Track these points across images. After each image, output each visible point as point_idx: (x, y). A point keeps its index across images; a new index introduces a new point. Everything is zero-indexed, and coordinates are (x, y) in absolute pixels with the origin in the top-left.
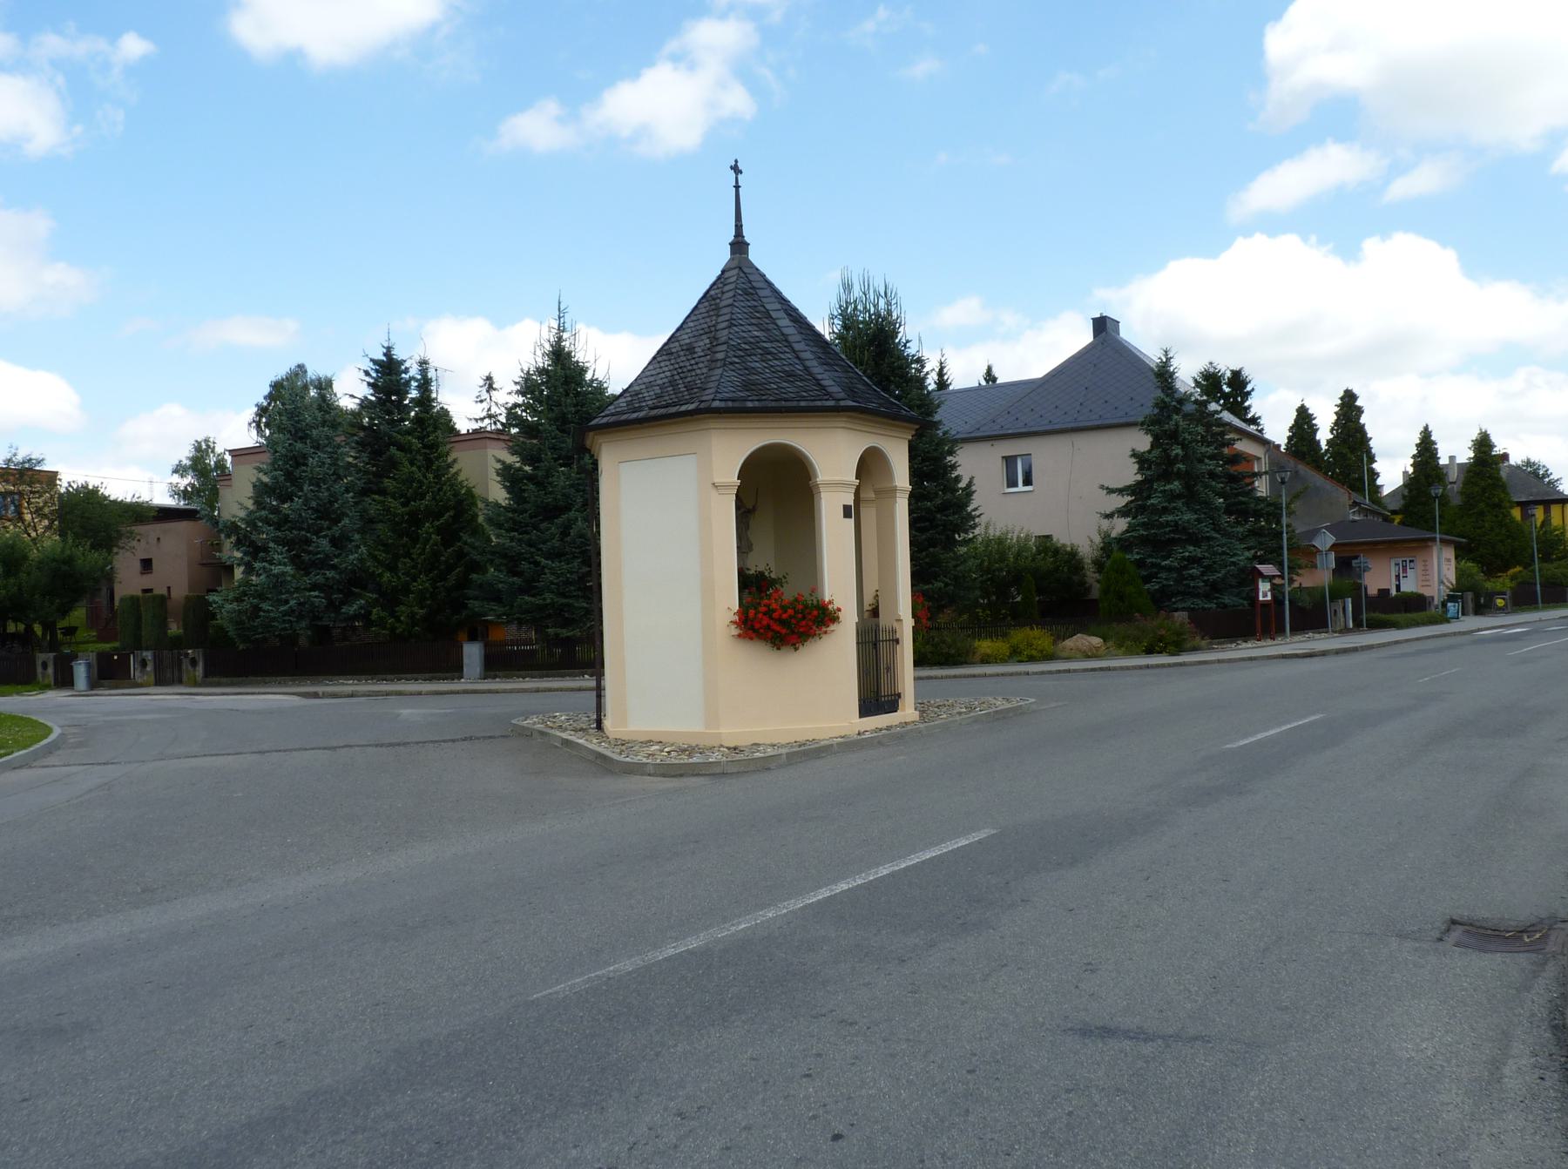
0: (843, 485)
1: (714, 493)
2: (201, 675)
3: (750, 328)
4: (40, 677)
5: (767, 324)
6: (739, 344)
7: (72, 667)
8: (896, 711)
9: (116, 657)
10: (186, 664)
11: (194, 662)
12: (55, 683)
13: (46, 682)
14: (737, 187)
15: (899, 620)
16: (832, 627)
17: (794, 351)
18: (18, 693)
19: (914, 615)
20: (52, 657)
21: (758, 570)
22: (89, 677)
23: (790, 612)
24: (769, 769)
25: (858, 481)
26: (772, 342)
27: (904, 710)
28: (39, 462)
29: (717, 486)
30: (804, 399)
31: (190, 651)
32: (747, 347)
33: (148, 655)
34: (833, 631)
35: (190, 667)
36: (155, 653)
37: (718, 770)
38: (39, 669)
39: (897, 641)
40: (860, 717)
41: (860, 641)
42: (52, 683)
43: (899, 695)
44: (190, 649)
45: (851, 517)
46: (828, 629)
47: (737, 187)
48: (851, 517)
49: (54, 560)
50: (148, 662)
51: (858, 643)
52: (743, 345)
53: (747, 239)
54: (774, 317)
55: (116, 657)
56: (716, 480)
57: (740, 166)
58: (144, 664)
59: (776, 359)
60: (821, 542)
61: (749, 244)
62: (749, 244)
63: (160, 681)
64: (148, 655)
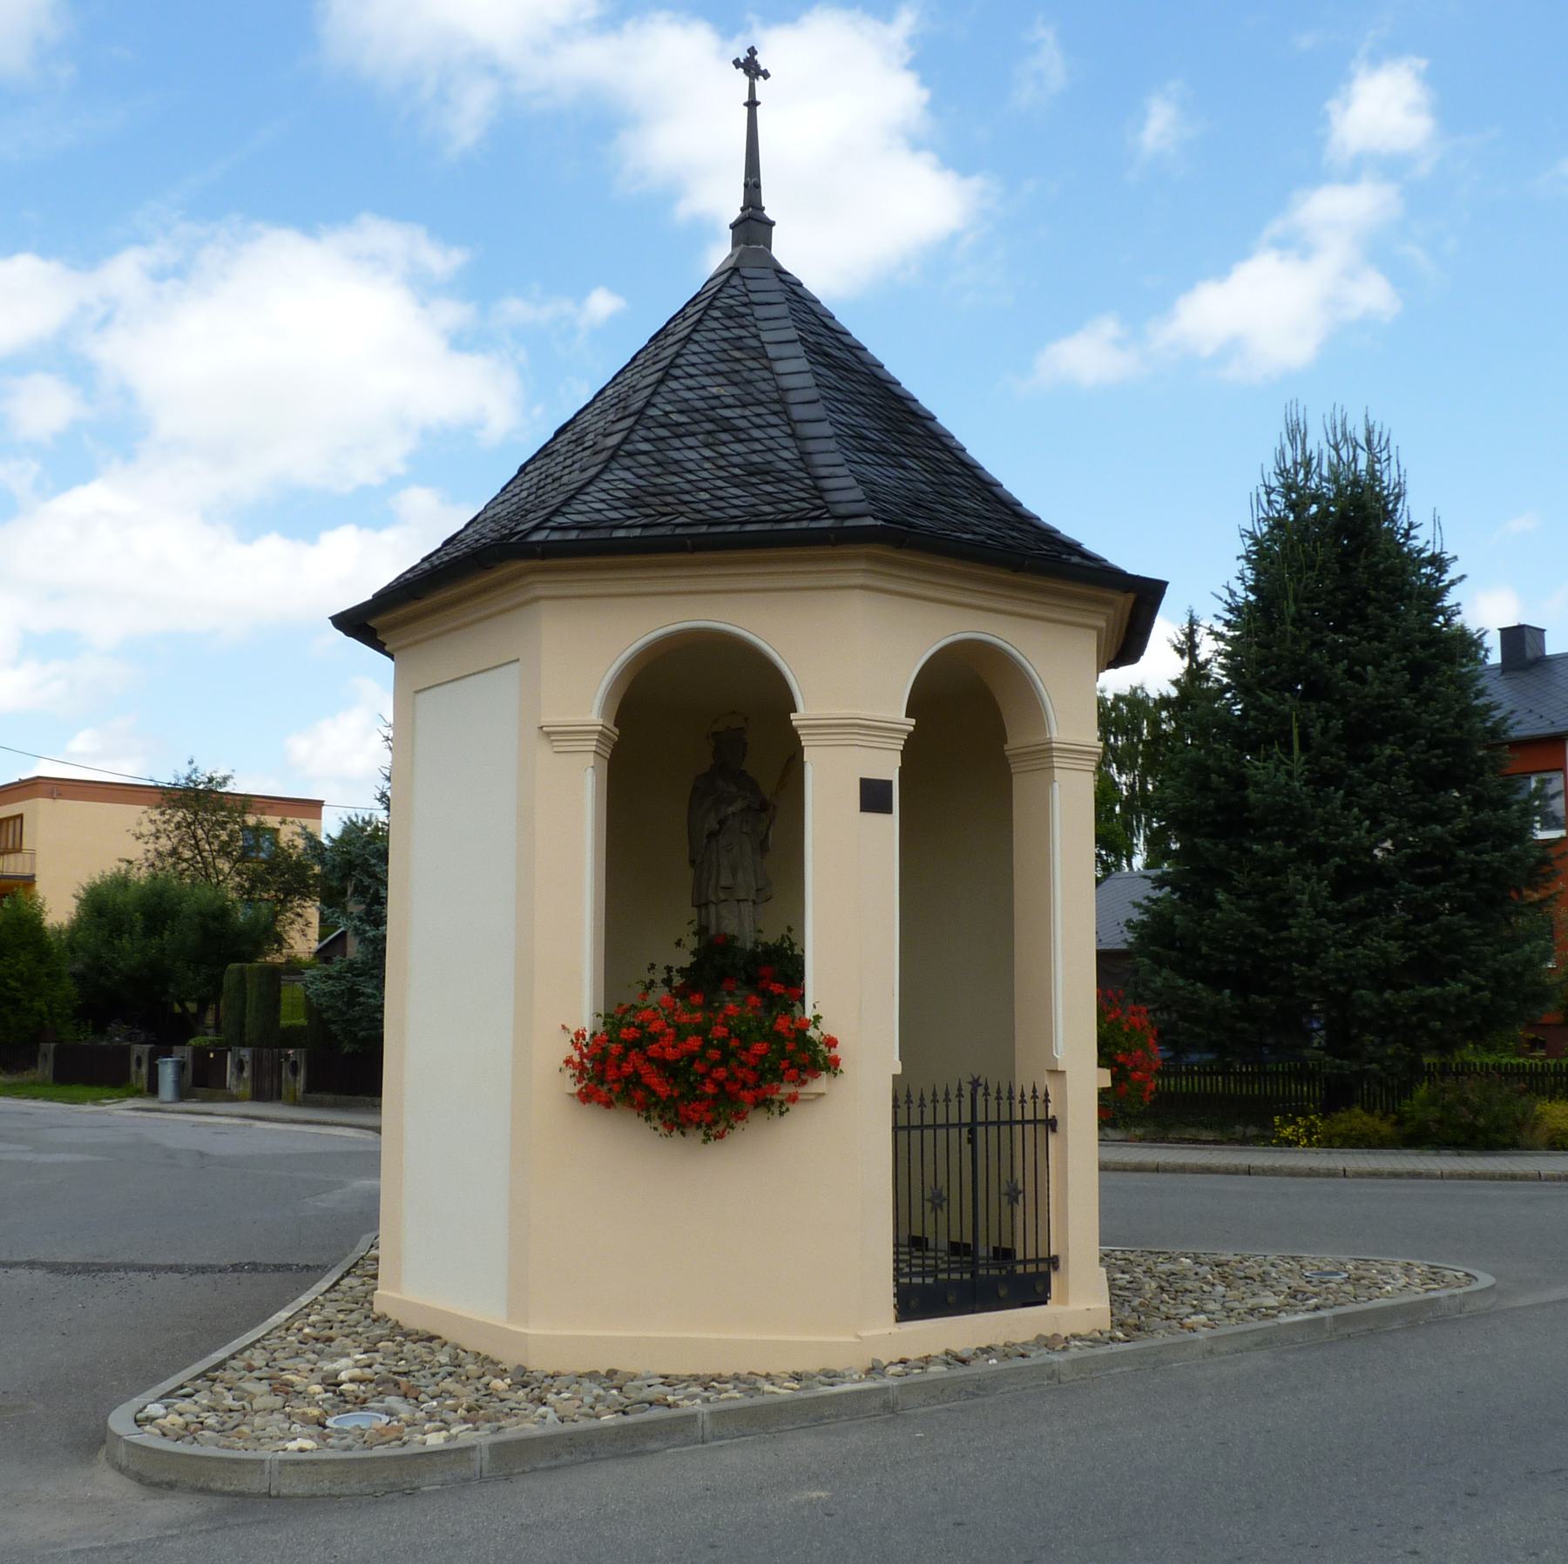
0: (874, 729)
1: (543, 753)
2: (302, 1089)
3: (706, 381)
4: (133, 1078)
5: (752, 370)
6: (666, 414)
7: (157, 1065)
8: (1045, 1303)
9: (212, 1055)
10: (286, 1073)
11: (294, 1069)
12: (148, 1088)
13: (139, 1086)
14: (752, 104)
15: (1057, 1073)
16: (820, 1084)
17: (790, 422)
18: (95, 1101)
19: (1106, 1056)
20: (147, 1050)
21: (764, 938)
22: (178, 1083)
23: (694, 1042)
24: (413, 1492)
25: (913, 721)
26: (744, 406)
27: (1064, 1300)
28: (225, 779)
29: (548, 734)
30: (759, 517)
31: (291, 1052)
32: (682, 419)
33: (246, 1054)
34: (821, 1095)
35: (290, 1076)
36: (253, 1051)
37: (255, 1484)
38: (133, 1068)
39: (1052, 1124)
40: (898, 1320)
41: (903, 1122)
42: (146, 1089)
43: (1054, 1262)
44: (290, 1048)
45: (889, 810)
46: (802, 1090)
47: (752, 104)
48: (889, 810)
49: (200, 913)
50: (246, 1065)
51: (896, 1128)
52: (674, 416)
53: (769, 213)
54: (771, 355)
55: (212, 1055)
56: (545, 720)
57: (763, 61)
58: (240, 1067)
59: (740, 441)
60: (596, 851)
61: (772, 224)
62: (772, 224)
63: (259, 1095)
64: (246, 1054)
